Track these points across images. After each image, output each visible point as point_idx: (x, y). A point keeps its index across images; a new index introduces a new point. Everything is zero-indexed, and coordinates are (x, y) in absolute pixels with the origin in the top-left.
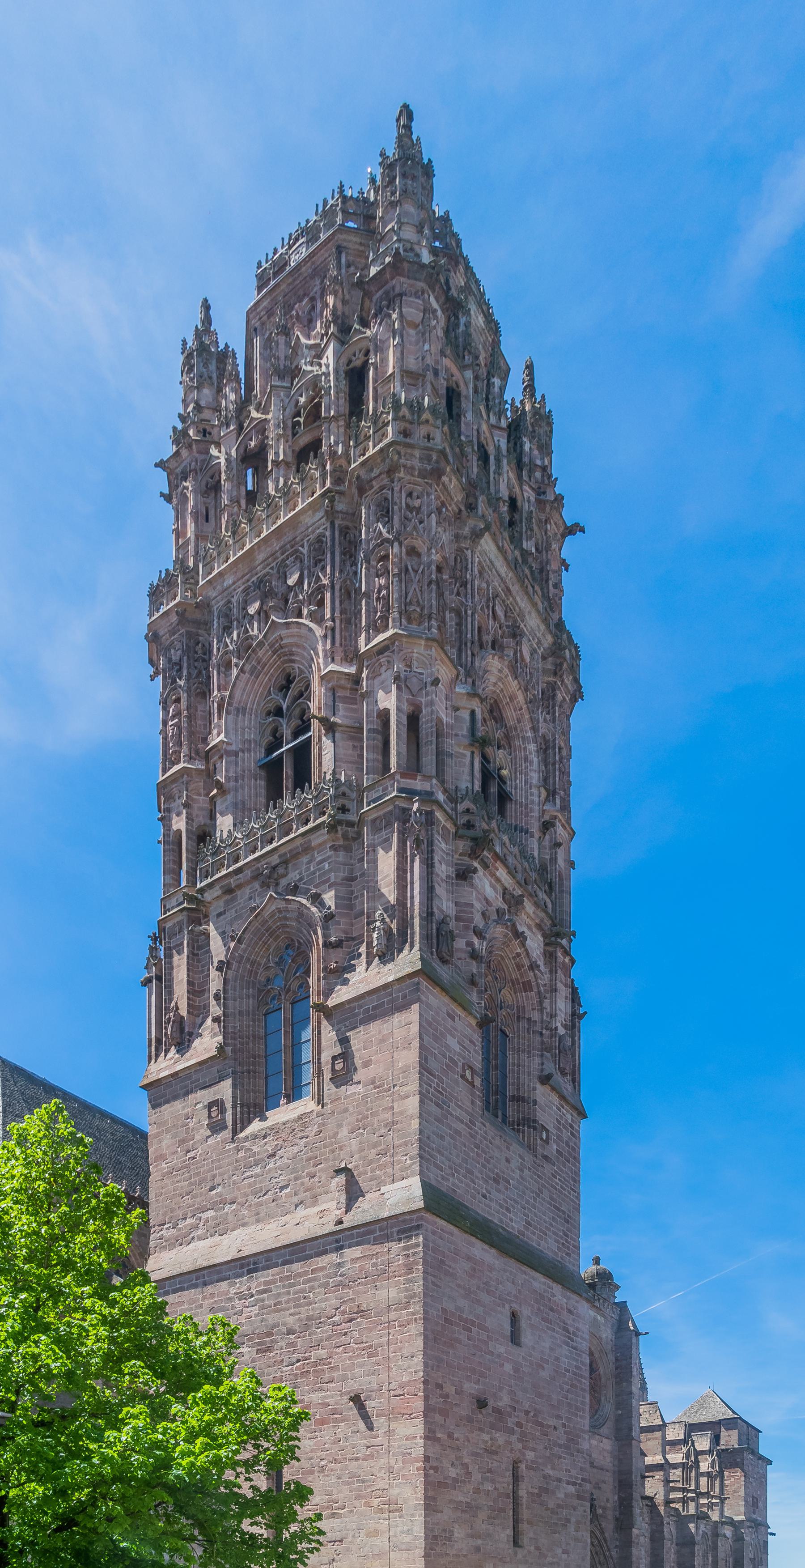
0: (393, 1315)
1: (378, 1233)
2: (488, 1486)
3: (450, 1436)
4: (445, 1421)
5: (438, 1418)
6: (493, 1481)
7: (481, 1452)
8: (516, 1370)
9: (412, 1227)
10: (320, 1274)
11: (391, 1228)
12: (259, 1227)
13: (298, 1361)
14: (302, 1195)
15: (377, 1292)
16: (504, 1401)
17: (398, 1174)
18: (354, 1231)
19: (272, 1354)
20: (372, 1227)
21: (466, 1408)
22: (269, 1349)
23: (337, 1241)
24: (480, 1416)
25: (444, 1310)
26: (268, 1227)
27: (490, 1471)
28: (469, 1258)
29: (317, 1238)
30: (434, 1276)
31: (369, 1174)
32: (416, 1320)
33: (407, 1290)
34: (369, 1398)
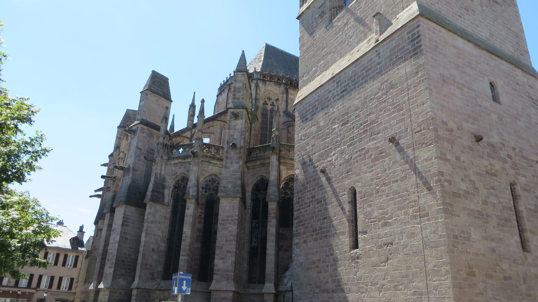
0: (409, 82)
1: (397, 39)
2: (493, 200)
3: (458, 158)
4: (452, 147)
5: (446, 144)
6: (496, 196)
7: (484, 173)
8: (500, 119)
9: (415, 28)
10: (370, 72)
11: (404, 33)
12: (342, 60)
13: (361, 125)
14: (360, 36)
15: (399, 72)
16: (495, 139)
17: (404, 5)
18: (385, 43)
19: (349, 125)
20: (393, 37)
21: (467, 141)
22: (347, 122)
23: (377, 51)
24: (478, 147)
25: (442, 75)
26: (345, 58)
27: (493, 188)
28: (454, 47)
29: (366, 53)
30: (432, 54)
31: (390, 12)
32: (423, 80)
33: (416, 64)
34: (400, 138)
